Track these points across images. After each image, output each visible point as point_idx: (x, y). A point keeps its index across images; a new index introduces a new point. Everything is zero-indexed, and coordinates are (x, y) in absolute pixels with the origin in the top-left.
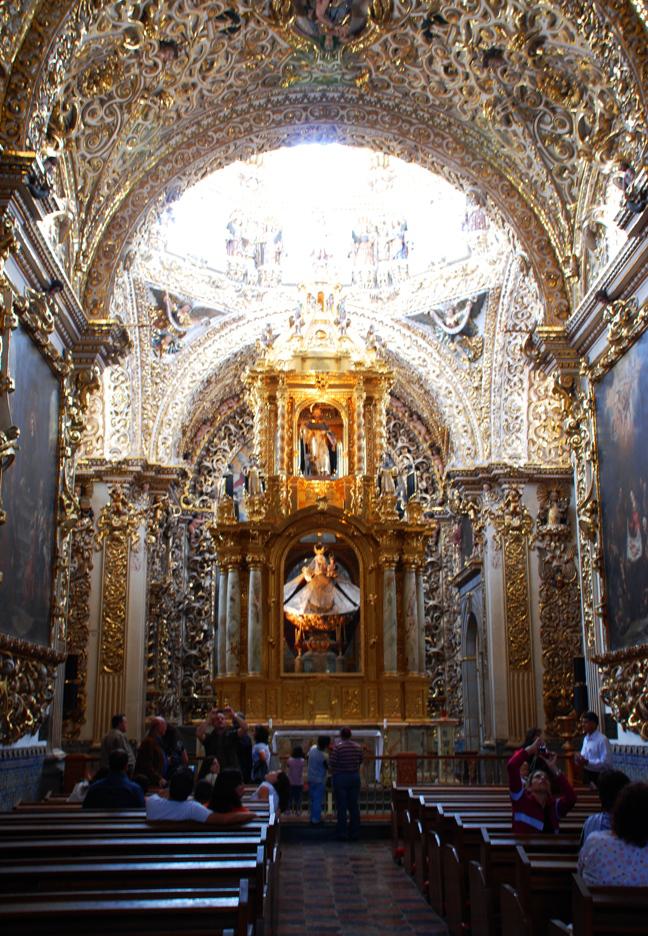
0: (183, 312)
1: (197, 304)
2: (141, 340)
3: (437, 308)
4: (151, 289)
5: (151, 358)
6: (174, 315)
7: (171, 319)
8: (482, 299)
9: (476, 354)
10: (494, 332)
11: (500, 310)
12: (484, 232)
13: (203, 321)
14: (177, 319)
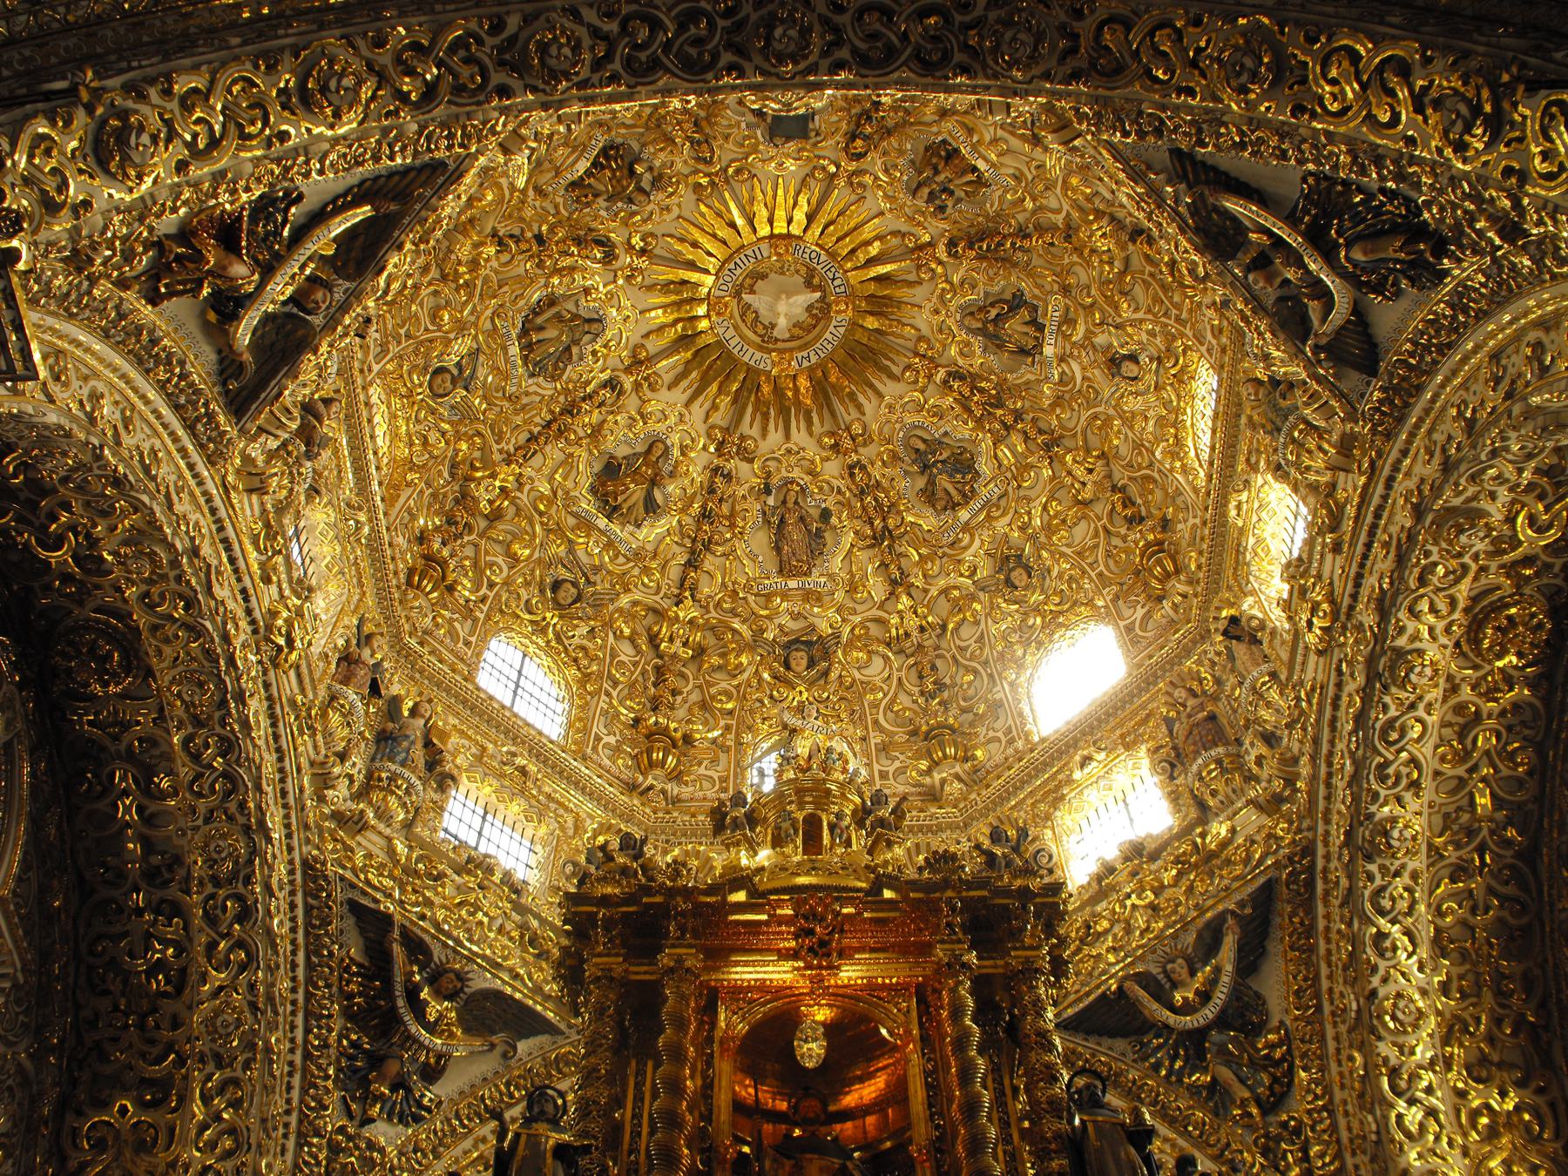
0: (440, 995)
1: (483, 981)
2: (307, 1056)
3: (1139, 969)
4: (354, 907)
5: (332, 1119)
6: (412, 993)
7: (400, 1002)
8: (1265, 897)
9: (1275, 1080)
10: (1317, 996)
11: (1321, 923)
12: (1232, 749)
13: (495, 1039)
14: (418, 1008)
